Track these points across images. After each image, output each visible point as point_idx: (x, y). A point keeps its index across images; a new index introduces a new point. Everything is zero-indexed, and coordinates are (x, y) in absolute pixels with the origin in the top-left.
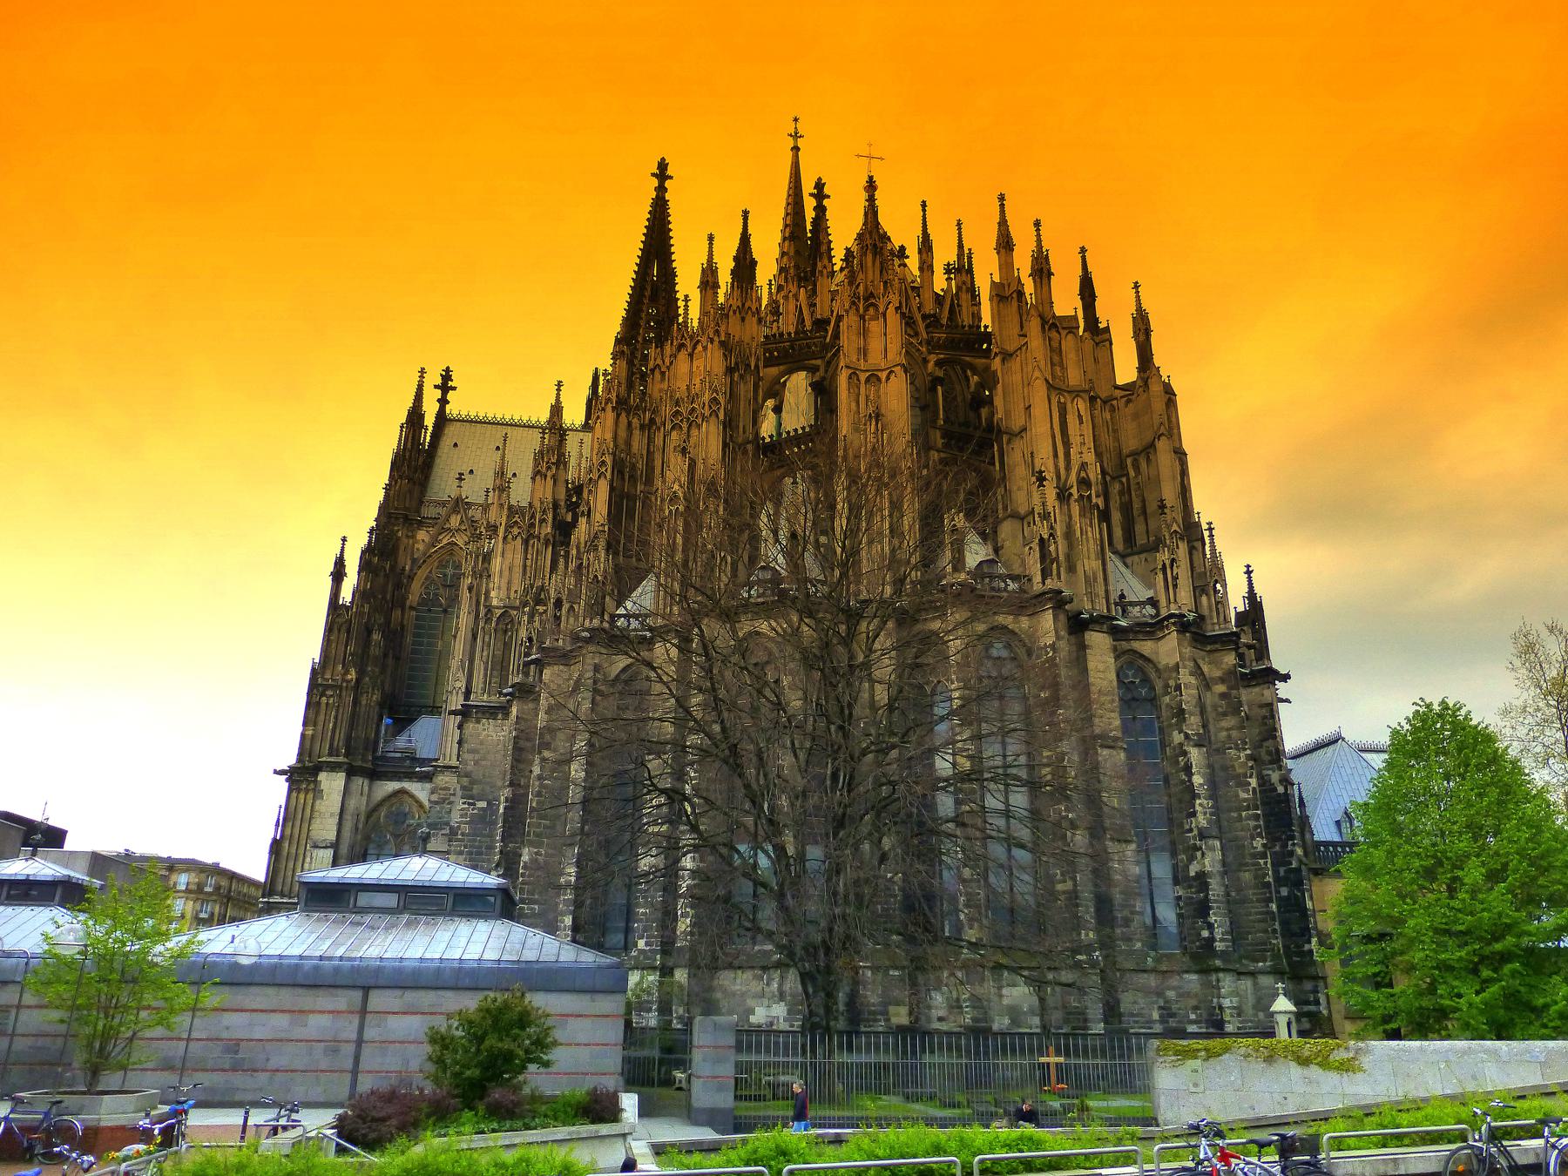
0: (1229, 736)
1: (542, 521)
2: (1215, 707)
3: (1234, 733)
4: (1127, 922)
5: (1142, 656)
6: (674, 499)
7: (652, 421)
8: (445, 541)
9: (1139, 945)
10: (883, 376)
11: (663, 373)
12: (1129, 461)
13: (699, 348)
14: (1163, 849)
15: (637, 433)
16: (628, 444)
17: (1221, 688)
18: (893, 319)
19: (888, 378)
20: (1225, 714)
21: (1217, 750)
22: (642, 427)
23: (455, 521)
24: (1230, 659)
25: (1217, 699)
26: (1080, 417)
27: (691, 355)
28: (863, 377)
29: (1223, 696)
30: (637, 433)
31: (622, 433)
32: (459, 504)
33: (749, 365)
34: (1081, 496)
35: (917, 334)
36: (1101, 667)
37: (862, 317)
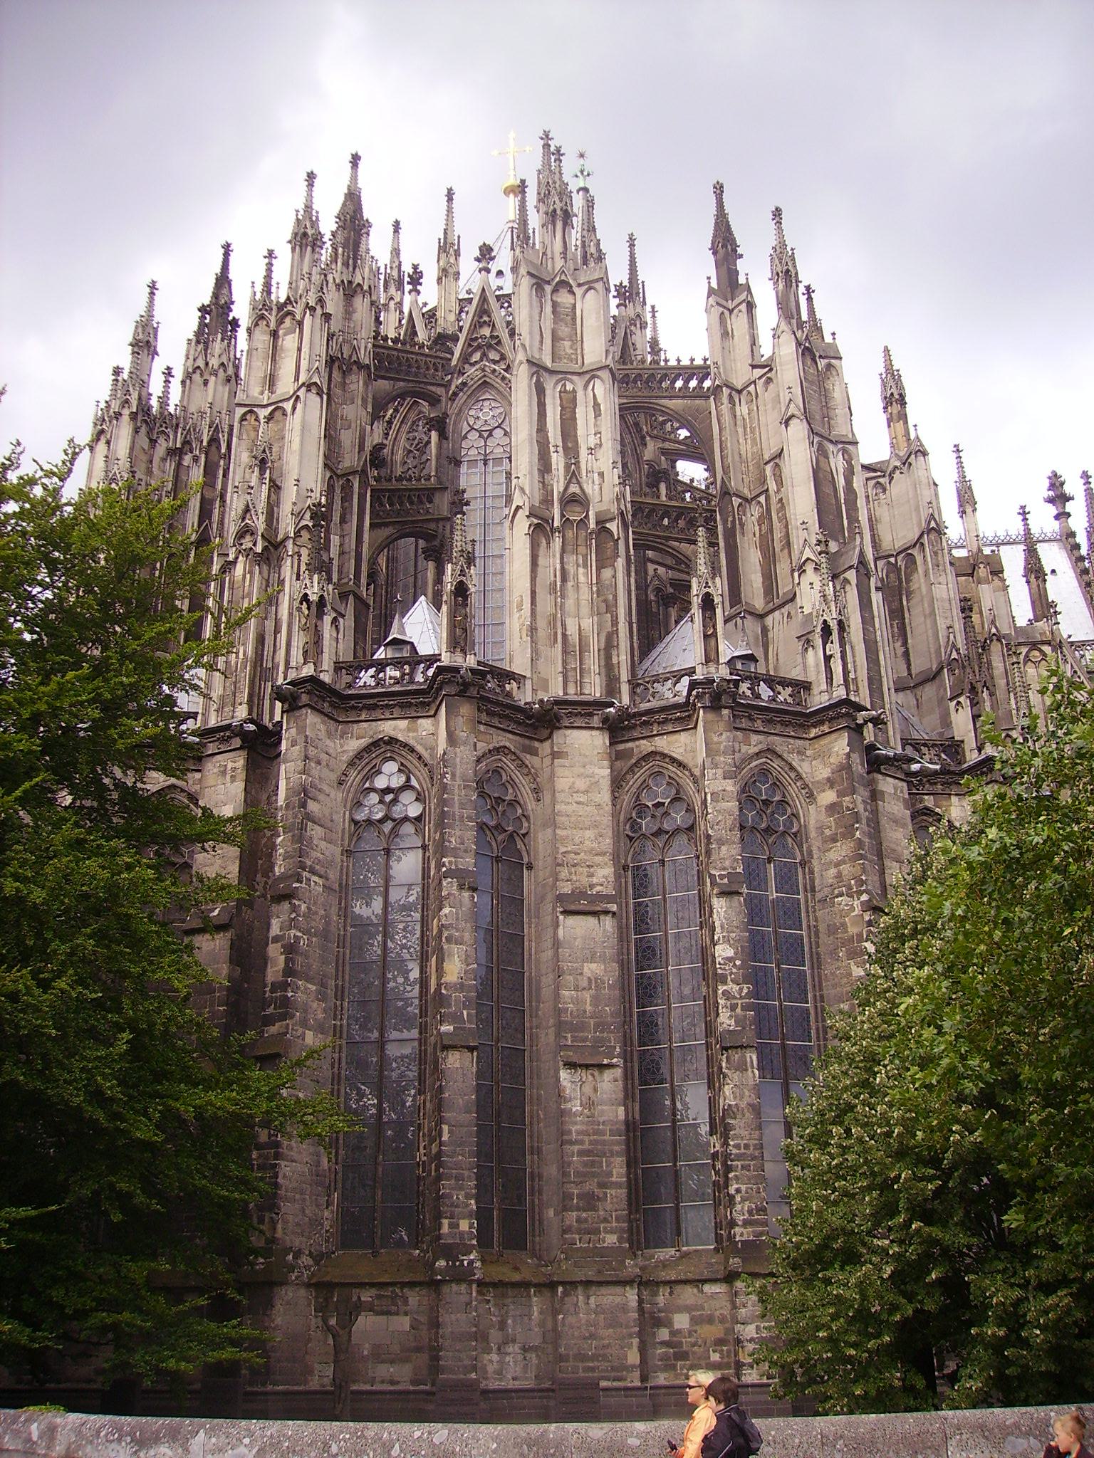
0: (839, 876)
2: (820, 829)
3: (846, 869)
4: (590, 1201)
5: (673, 760)
9: (611, 1239)
10: (288, 406)
14: (697, 1076)
17: (829, 797)
19: (294, 408)
20: (834, 840)
21: (823, 901)
24: (840, 745)
25: (823, 816)
26: (596, 406)
29: (832, 808)
34: (566, 522)
36: (581, 784)
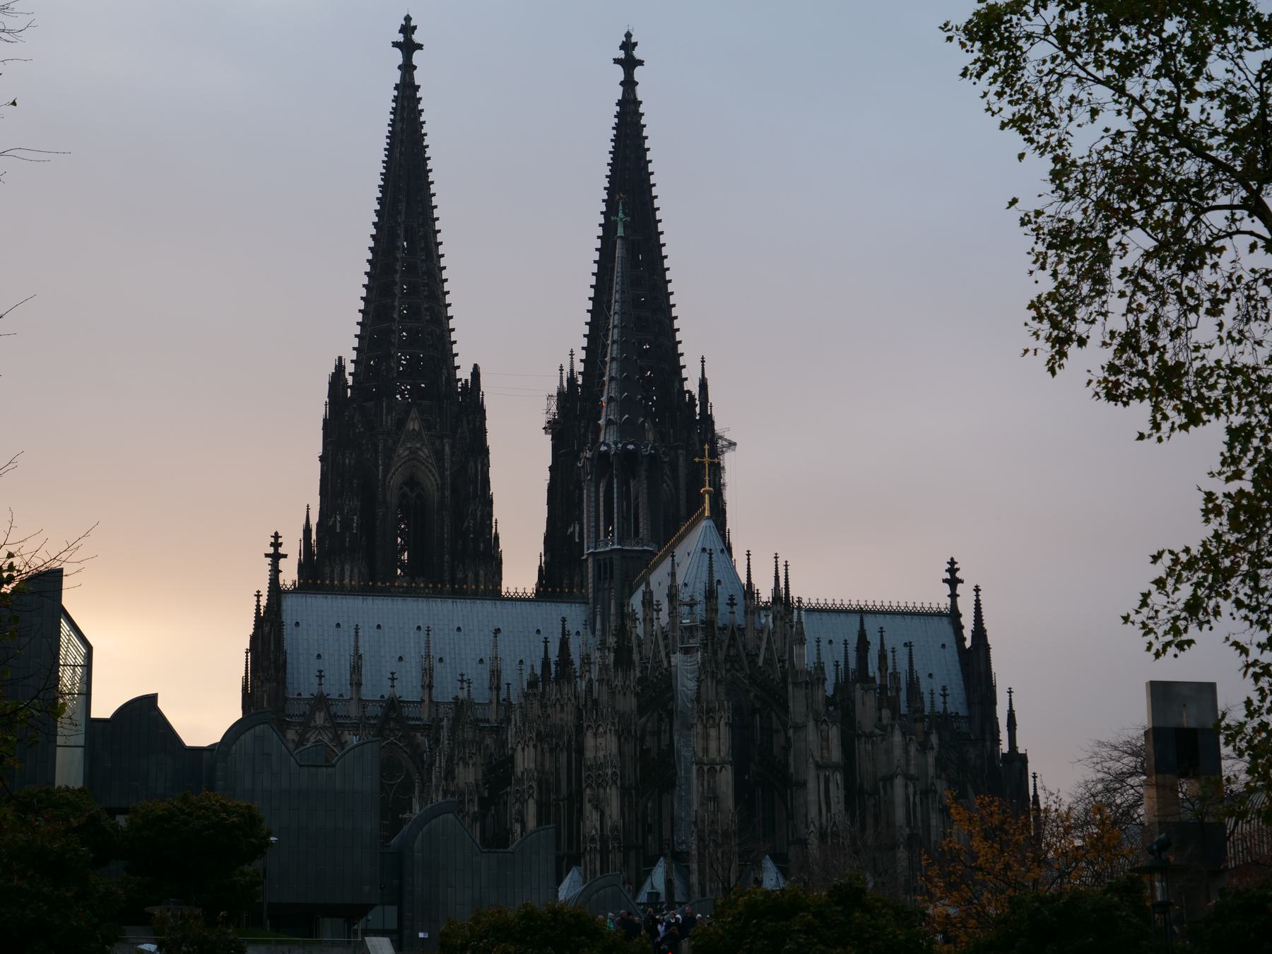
1: (471, 801)
6: (593, 840)
7: (557, 744)
8: (312, 740)
10: (718, 768)
11: (562, 706)
12: (881, 784)
13: (601, 730)
15: (547, 755)
16: (543, 765)
18: (724, 731)
22: (551, 750)
23: (320, 718)
27: (595, 735)
28: (706, 768)
30: (547, 755)
31: (539, 758)
32: (321, 701)
33: (630, 732)
35: (742, 669)
37: (705, 727)
